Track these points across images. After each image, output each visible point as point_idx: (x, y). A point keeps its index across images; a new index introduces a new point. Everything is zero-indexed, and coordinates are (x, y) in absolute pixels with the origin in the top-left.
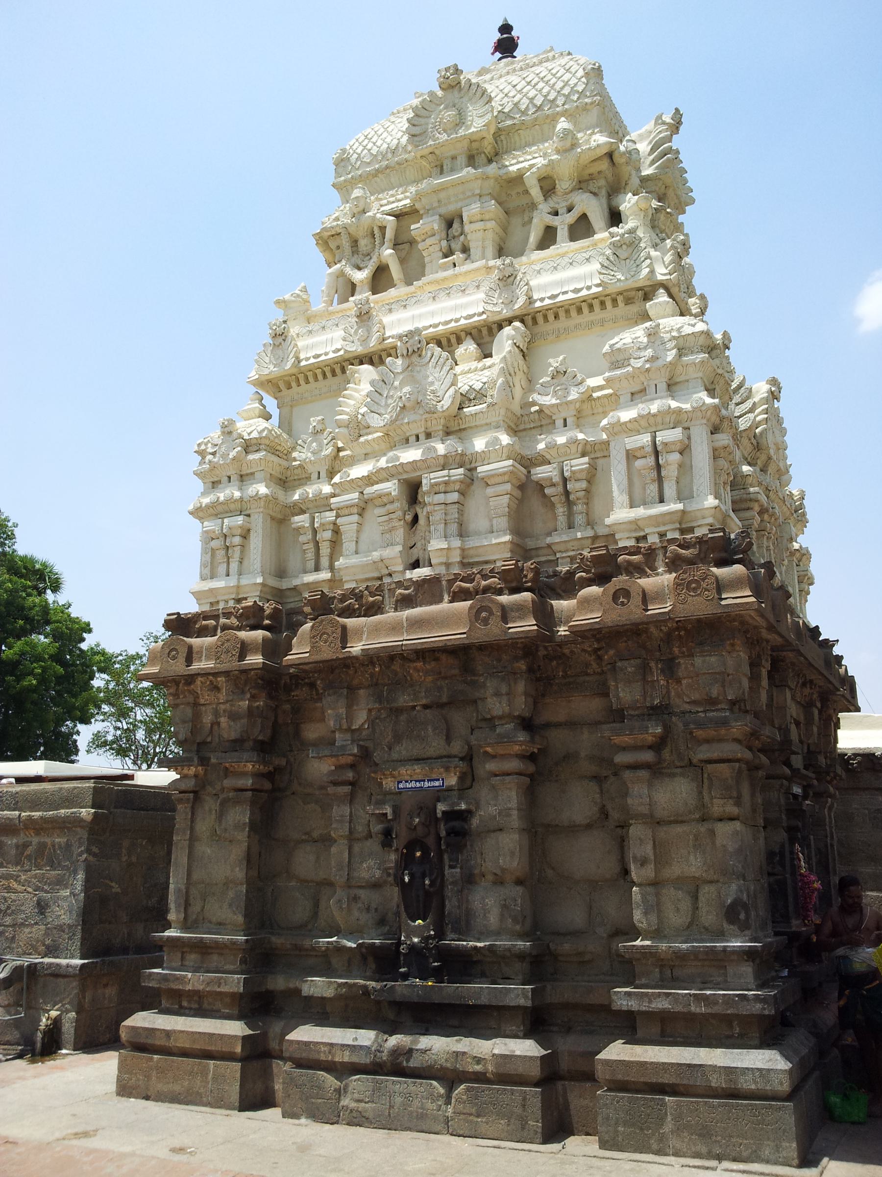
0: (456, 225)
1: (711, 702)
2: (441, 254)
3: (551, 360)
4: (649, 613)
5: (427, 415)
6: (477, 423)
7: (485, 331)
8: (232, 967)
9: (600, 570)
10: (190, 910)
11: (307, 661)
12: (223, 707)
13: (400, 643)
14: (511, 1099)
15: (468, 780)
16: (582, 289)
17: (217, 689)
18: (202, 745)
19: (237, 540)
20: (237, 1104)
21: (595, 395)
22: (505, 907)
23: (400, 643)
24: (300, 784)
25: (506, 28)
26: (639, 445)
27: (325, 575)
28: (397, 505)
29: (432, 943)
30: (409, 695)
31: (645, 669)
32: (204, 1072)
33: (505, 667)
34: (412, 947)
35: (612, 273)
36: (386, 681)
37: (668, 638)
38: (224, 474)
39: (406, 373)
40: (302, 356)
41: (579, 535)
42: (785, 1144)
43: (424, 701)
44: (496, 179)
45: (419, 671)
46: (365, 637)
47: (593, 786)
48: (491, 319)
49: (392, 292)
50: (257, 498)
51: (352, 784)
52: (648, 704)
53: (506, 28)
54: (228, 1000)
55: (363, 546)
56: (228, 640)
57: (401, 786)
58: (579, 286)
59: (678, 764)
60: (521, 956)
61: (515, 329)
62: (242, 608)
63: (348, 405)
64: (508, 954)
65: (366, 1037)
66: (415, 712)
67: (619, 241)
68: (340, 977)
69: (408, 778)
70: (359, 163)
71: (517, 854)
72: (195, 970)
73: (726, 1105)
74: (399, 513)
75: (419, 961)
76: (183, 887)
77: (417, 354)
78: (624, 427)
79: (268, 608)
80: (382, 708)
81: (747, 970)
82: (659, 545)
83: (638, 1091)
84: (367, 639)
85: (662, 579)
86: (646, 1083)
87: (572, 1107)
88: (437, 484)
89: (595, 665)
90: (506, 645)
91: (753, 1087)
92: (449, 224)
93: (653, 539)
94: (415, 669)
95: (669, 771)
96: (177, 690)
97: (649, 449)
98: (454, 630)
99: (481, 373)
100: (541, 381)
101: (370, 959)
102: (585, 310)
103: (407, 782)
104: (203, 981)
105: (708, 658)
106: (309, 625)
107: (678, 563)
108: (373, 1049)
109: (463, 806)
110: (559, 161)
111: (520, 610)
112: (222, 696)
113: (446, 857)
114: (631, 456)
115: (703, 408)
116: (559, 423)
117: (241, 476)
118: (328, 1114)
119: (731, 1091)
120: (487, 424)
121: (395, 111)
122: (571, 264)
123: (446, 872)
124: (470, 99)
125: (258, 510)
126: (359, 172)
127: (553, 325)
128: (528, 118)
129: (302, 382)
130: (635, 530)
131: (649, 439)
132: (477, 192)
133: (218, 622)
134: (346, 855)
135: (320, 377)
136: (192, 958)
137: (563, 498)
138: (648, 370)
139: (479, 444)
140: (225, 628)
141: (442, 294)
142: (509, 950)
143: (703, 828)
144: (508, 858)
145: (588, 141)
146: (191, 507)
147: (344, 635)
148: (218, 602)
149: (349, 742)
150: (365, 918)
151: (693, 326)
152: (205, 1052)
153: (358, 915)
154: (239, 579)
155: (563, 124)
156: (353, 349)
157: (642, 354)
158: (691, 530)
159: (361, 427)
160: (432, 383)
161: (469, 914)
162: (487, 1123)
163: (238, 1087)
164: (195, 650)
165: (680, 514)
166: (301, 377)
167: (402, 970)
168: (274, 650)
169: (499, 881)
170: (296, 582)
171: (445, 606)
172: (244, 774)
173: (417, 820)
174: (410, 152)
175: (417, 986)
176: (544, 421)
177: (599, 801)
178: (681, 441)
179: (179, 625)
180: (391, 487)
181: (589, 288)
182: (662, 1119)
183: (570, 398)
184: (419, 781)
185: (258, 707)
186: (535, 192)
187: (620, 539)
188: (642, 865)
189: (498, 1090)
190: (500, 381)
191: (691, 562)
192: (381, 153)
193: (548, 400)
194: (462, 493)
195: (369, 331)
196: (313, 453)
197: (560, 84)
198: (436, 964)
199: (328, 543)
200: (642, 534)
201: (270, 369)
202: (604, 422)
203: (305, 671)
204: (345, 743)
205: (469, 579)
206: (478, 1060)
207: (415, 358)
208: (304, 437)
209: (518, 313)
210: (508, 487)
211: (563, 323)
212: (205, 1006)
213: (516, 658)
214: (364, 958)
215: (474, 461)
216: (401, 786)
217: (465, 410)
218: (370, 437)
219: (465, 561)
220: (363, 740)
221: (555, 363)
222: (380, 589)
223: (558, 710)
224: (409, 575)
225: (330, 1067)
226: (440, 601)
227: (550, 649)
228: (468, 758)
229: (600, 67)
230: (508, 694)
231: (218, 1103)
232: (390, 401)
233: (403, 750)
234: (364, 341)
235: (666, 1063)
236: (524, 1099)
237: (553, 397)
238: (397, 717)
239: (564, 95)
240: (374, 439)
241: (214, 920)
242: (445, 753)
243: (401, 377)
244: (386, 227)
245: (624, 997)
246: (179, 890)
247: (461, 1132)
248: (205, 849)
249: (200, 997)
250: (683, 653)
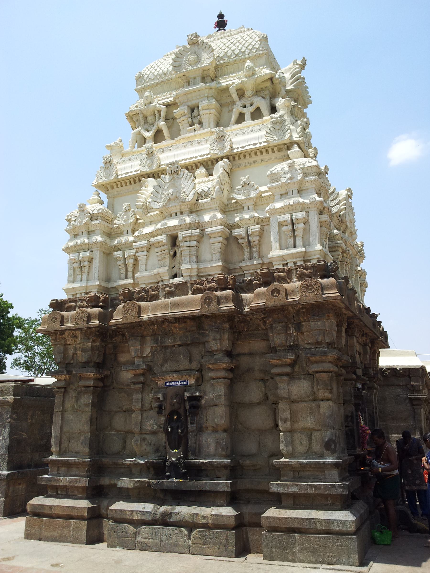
0: (196, 111)
1: (318, 343)
2: (188, 125)
3: (242, 178)
4: (289, 300)
5: (181, 203)
6: (206, 207)
7: (210, 163)
8: (83, 474)
9: (265, 280)
10: (62, 446)
11: (121, 323)
12: (78, 346)
13: (167, 314)
14: (220, 536)
15: (200, 381)
16: (257, 144)
17: (76, 337)
18: (68, 365)
19: (86, 263)
20: (85, 541)
21: (263, 195)
22: (218, 443)
23: (167, 314)
24: (117, 384)
25: (221, 16)
26: (284, 219)
27: (130, 281)
28: (166, 247)
29: (182, 461)
30: (171, 340)
31: (286, 328)
32: (69, 526)
33: (219, 326)
34: (172, 463)
35: (272, 136)
36: (160, 333)
37: (298, 313)
38: (80, 231)
39: (171, 183)
40: (119, 173)
41: (255, 263)
42: (352, 556)
43: (179, 343)
44: (216, 89)
45: (176, 328)
46: (150, 311)
47: (261, 384)
48: (213, 157)
49: (164, 143)
50: (96, 243)
51: (143, 383)
52: (288, 345)
53: (221, 16)
54: (81, 490)
55: (149, 267)
56: (81, 313)
57: (167, 384)
58: (256, 142)
59: (302, 374)
60: (226, 467)
61: (225, 162)
62: (89, 297)
63: (142, 198)
64: (219, 466)
65: (149, 507)
66: (174, 348)
67: (275, 121)
68: (136, 478)
69: (170, 380)
70: (148, 79)
71: (224, 417)
72: (64, 476)
73: (325, 537)
74: (167, 251)
75: (175, 469)
76: (59, 435)
77: (176, 174)
78: (277, 211)
79: (102, 297)
80: (158, 346)
81: (335, 472)
82: (294, 268)
83: (282, 532)
84: (151, 312)
85: (295, 284)
86: (286, 528)
87: (250, 540)
88: (186, 237)
89: (262, 326)
90: (219, 316)
91: (338, 529)
92: (193, 110)
93: (291, 265)
94: (175, 327)
95: (298, 377)
96: (56, 337)
97: (289, 222)
98: (194, 308)
99: (207, 183)
100: (237, 188)
101: (151, 469)
102: (259, 154)
103: (170, 382)
104: (68, 481)
105: (317, 322)
106: (122, 306)
107: (303, 276)
108: (153, 513)
109: (198, 394)
110: (246, 81)
111: (226, 299)
112: (79, 340)
113: (189, 419)
114: (280, 225)
115: (315, 202)
116: (246, 208)
117: (89, 232)
118: (130, 545)
119: (327, 531)
120: (210, 208)
121: (166, 54)
122: (252, 131)
123: (189, 426)
124: (203, 50)
125: (97, 249)
126: (148, 84)
127: (243, 161)
128: (231, 60)
129: (119, 186)
130: (282, 261)
131: (289, 217)
132: (206, 95)
133: (76, 304)
134: (140, 418)
135: (128, 183)
136: (63, 470)
137: (248, 245)
138: (289, 184)
139: (207, 218)
140: (80, 307)
141: (189, 144)
142: (220, 464)
143: (314, 404)
144: (219, 419)
145: (260, 72)
146: (63, 247)
147: (139, 310)
148: (76, 294)
149: (142, 363)
150: (149, 449)
151: (311, 162)
152: (69, 516)
153: (145, 448)
154: (87, 283)
155: (248, 63)
156: (145, 170)
157: (286, 176)
158: (309, 261)
159: (148, 208)
160: (184, 188)
161: (200, 447)
162: (208, 548)
163: (85, 533)
164: (65, 318)
165: (303, 253)
167: (167, 474)
168: (105, 317)
169: (215, 430)
170: (116, 284)
171: (189, 296)
172: (89, 379)
173: (175, 401)
174: (173, 75)
175: (174, 482)
176: (238, 207)
177: (264, 391)
178: (304, 218)
179: (57, 305)
180: (163, 238)
181: (260, 143)
182: (294, 545)
183: (251, 196)
184: (176, 382)
185: (96, 346)
186: (235, 96)
187: (275, 265)
188: (284, 422)
189: (214, 532)
190: (217, 187)
191: (309, 276)
192: (159, 75)
193: (240, 197)
194: (198, 242)
195: (152, 162)
196: (125, 221)
197: (247, 44)
198: (184, 471)
199: (132, 265)
200: (286, 262)
201: (103, 179)
202: (268, 208)
203: (119, 328)
204: (139, 363)
205: (201, 283)
206: (204, 518)
207: (175, 175)
208: (120, 213)
209: (226, 155)
210: (221, 239)
211: (248, 160)
212: (69, 493)
213: (224, 322)
214: (148, 468)
215: (204, 226)
216: (167, 384)
217: (200, 201)
218: (153, 214)
219: (199, 274)
220: (148, 362)
221: (244, 179)
222: (157, 288)
223: (244, 347)
224: (172, 281)
225: (131, 522)
226: (187, 294)
227: (241, 317)
228: (200, 370)
229: (266, 36)
230: (220, 339)
231: (75, 541)
232: (163, 196)
233: (168, 367)
234: (150, 166)
235: (296, 518)
236: (227, 536)
237: (243, 195)
238: (165, 350)
239: (249, 49)
240: (155, 215)
241: (74, 451)
242: (189, 368)
243: (168, 184)
244: (161, 111)
245: (276, 486)
246: (57, 436)
247: (196, 553)
248: (69, 416)
249: (66, 489)
250: (305, 320)
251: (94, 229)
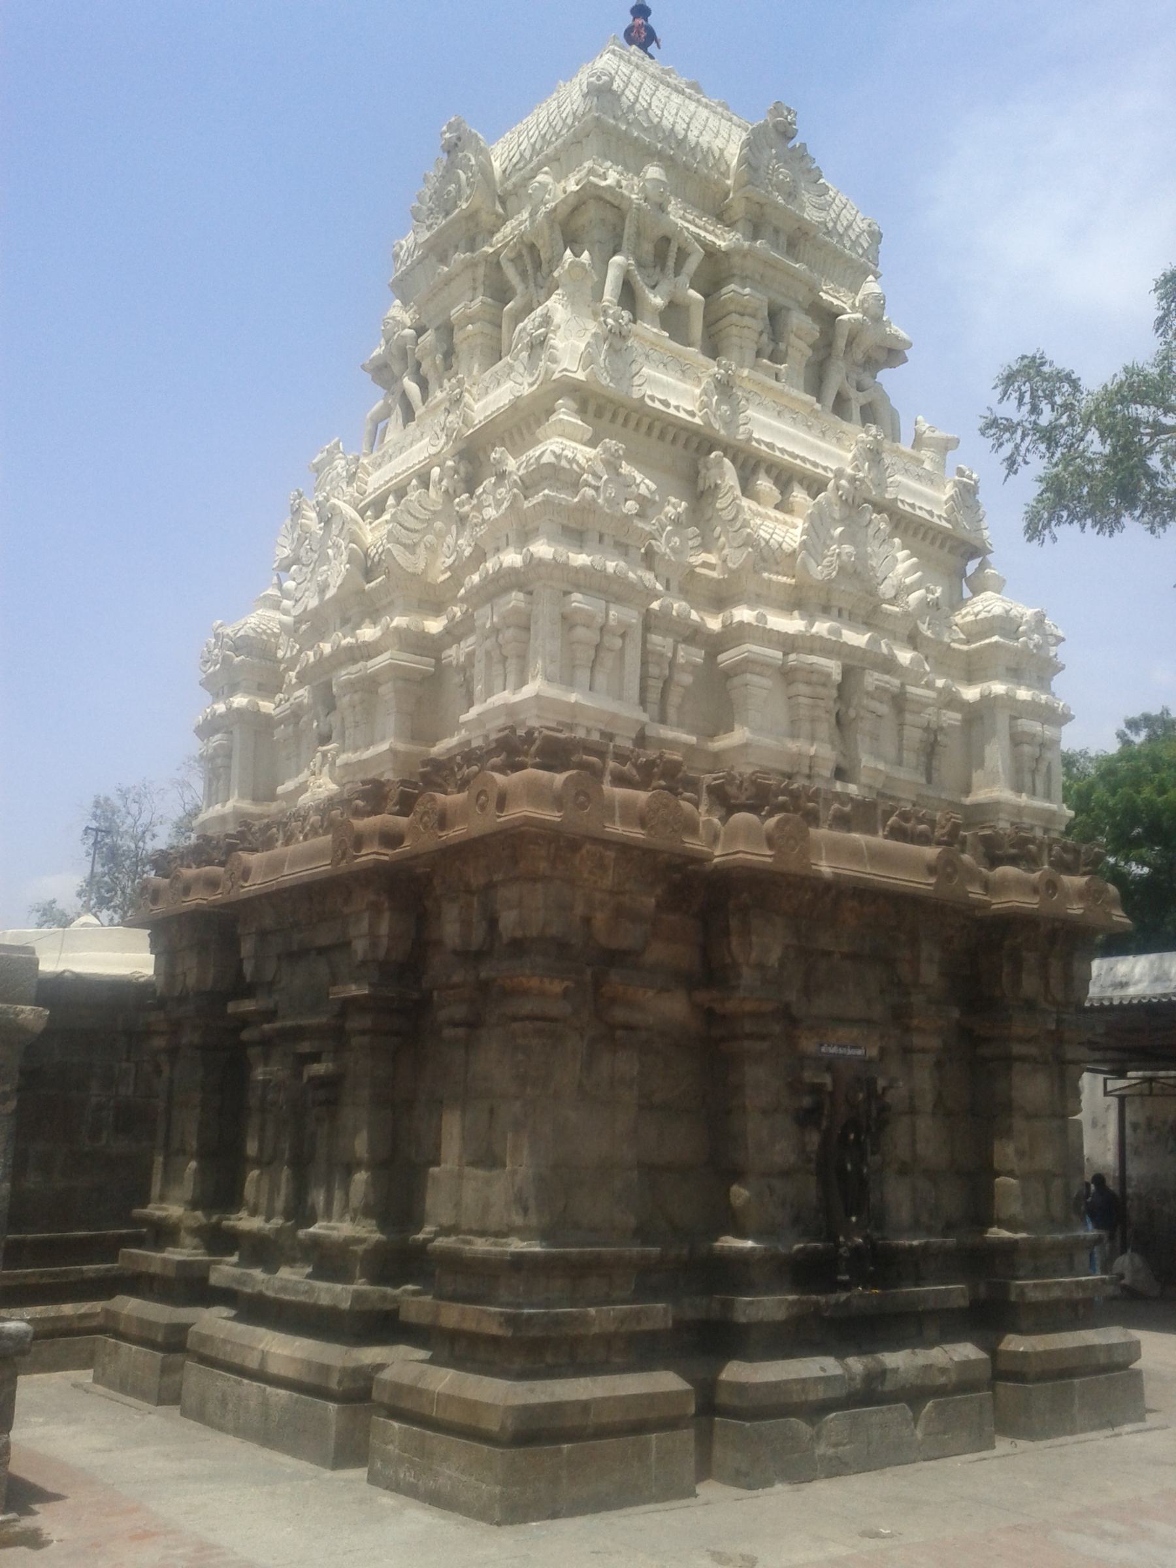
25: (641, 11)
34: (856, 1250)
53: (641, 11)
56: (666, 806)
57: (823, 1050)
118: (800, 1469)
133: (604, 762)
138: (1034, 655)
141: (787, 415)
152: (639, 1422)
166: (622, 414)
169: (904, 1170)
171: (878, 840)
180: (833, 667)
196: (673, 549)
206: (943, 1371)
218: (774, 577)
226: (874, 832)
240: (778, 583)
251: (629, 542)
